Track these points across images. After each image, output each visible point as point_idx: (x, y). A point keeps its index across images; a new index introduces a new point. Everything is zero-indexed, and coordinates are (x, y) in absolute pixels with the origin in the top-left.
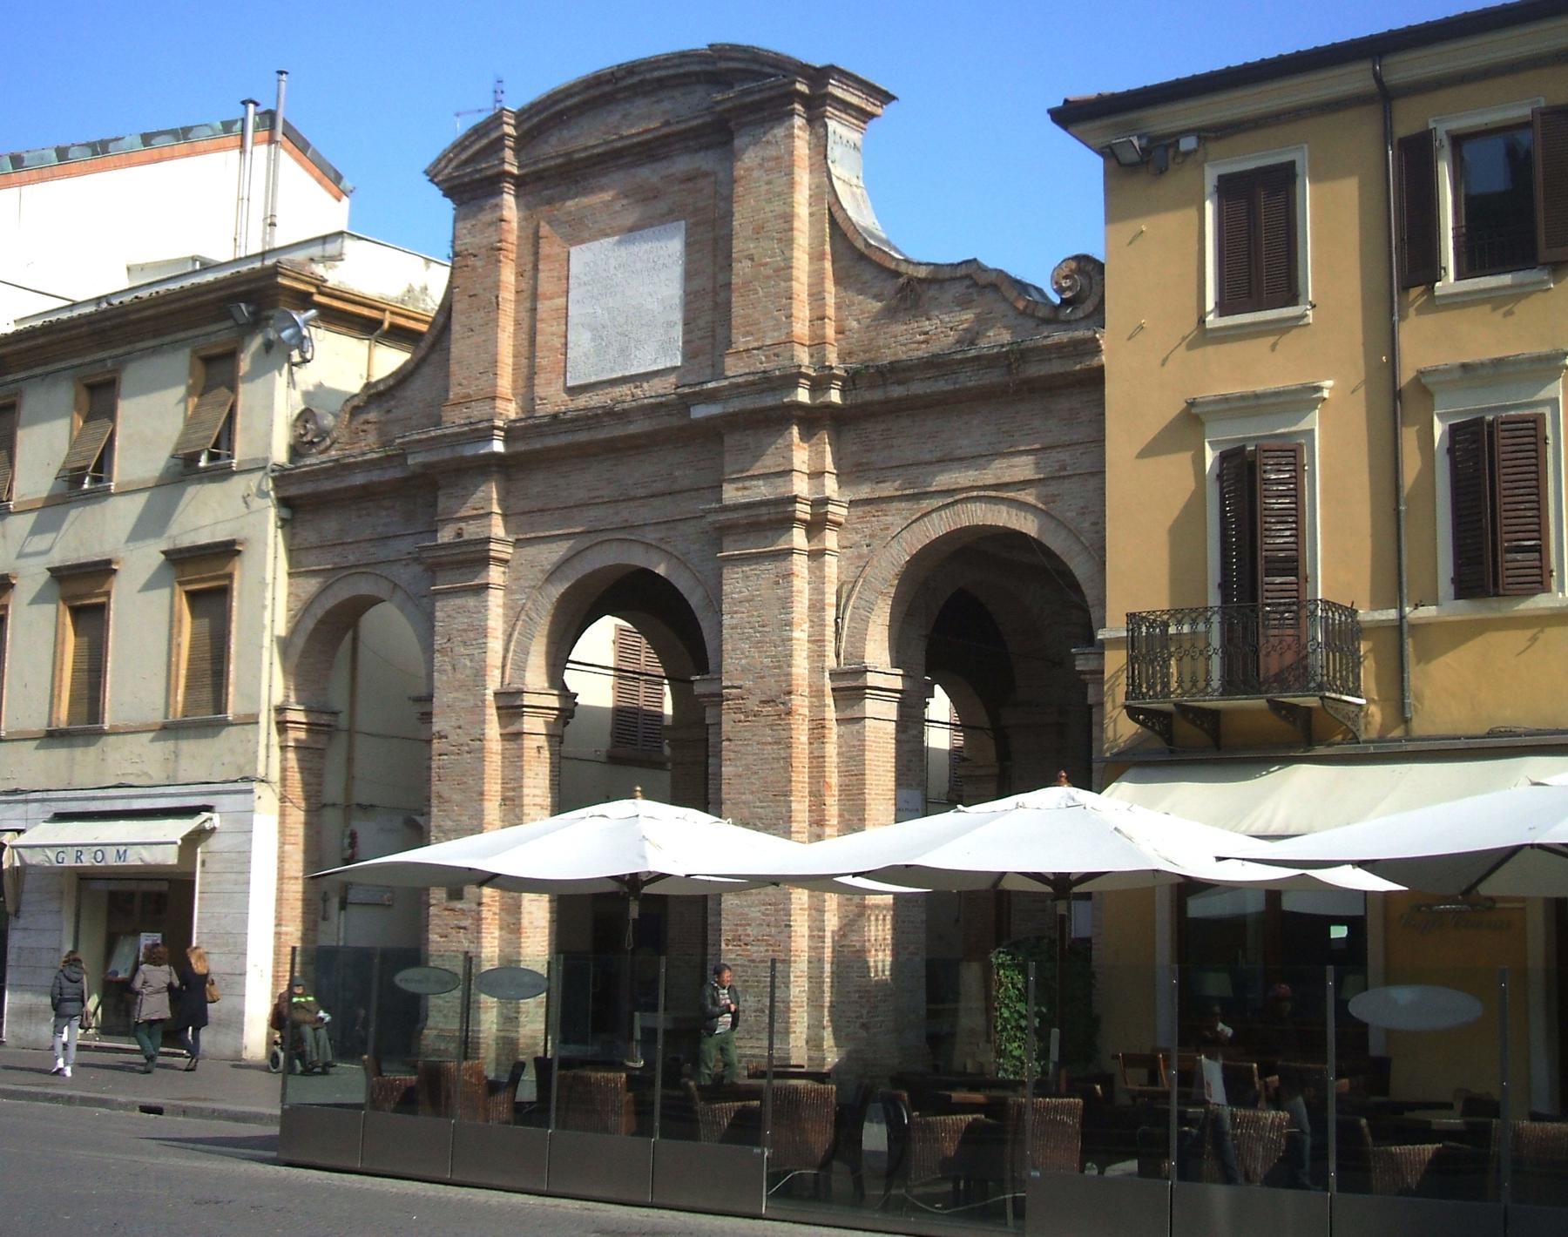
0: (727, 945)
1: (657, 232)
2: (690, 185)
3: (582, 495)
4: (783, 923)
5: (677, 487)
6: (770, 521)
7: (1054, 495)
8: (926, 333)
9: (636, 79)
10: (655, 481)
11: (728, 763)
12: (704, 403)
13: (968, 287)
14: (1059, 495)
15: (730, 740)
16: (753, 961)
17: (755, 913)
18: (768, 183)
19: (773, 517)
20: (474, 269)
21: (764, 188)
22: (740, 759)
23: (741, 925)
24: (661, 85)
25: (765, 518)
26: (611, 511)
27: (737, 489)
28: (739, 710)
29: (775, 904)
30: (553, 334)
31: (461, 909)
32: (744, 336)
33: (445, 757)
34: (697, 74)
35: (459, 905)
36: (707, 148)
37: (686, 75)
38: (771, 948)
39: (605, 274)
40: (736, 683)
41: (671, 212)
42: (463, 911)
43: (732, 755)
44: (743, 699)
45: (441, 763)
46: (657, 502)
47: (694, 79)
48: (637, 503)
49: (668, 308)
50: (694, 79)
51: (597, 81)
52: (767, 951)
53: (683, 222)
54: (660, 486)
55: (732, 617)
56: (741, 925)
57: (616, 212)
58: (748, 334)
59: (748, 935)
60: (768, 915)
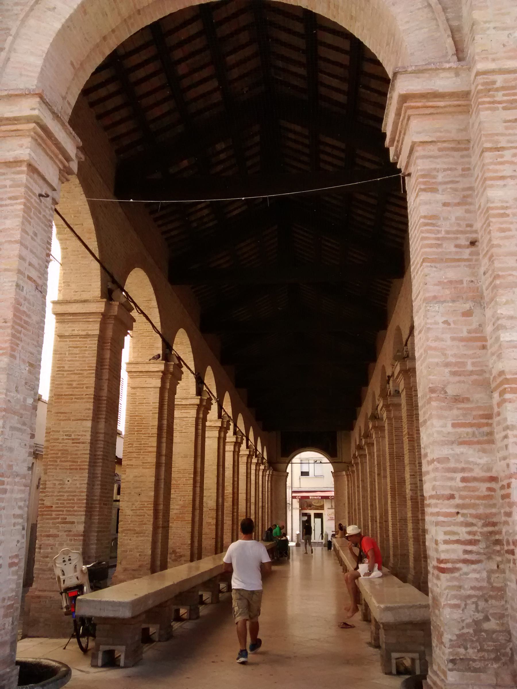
11: (501, 183)
15: (498, 149)
43: (507, 170)
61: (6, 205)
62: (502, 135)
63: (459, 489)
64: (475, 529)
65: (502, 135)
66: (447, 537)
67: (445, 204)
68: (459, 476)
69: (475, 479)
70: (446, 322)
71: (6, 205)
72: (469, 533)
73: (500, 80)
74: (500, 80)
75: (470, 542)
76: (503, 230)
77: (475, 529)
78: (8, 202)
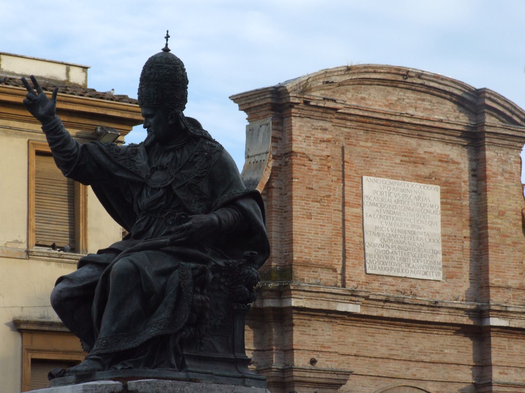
1: (426, 188)
2: (445, 165)
3: (383, 351)
5: (446, 360)
9: (419, 81)
10: (432, 353)
18: (507, 186)
20: (310, 169)
21: (504, 189)
24: (429, 90)
26: (404, 366)
30: (354, 233)
32: (496, 277)
34: (452, 94)
36: (454, 144)
39: (388, 203)
46: (434, 367)
48: (421, 364)
49: (432, 241)
51: (398, 71)
53: (439, 187)
54: (436, 358)
57: (396, 163)
58: (498, 276)
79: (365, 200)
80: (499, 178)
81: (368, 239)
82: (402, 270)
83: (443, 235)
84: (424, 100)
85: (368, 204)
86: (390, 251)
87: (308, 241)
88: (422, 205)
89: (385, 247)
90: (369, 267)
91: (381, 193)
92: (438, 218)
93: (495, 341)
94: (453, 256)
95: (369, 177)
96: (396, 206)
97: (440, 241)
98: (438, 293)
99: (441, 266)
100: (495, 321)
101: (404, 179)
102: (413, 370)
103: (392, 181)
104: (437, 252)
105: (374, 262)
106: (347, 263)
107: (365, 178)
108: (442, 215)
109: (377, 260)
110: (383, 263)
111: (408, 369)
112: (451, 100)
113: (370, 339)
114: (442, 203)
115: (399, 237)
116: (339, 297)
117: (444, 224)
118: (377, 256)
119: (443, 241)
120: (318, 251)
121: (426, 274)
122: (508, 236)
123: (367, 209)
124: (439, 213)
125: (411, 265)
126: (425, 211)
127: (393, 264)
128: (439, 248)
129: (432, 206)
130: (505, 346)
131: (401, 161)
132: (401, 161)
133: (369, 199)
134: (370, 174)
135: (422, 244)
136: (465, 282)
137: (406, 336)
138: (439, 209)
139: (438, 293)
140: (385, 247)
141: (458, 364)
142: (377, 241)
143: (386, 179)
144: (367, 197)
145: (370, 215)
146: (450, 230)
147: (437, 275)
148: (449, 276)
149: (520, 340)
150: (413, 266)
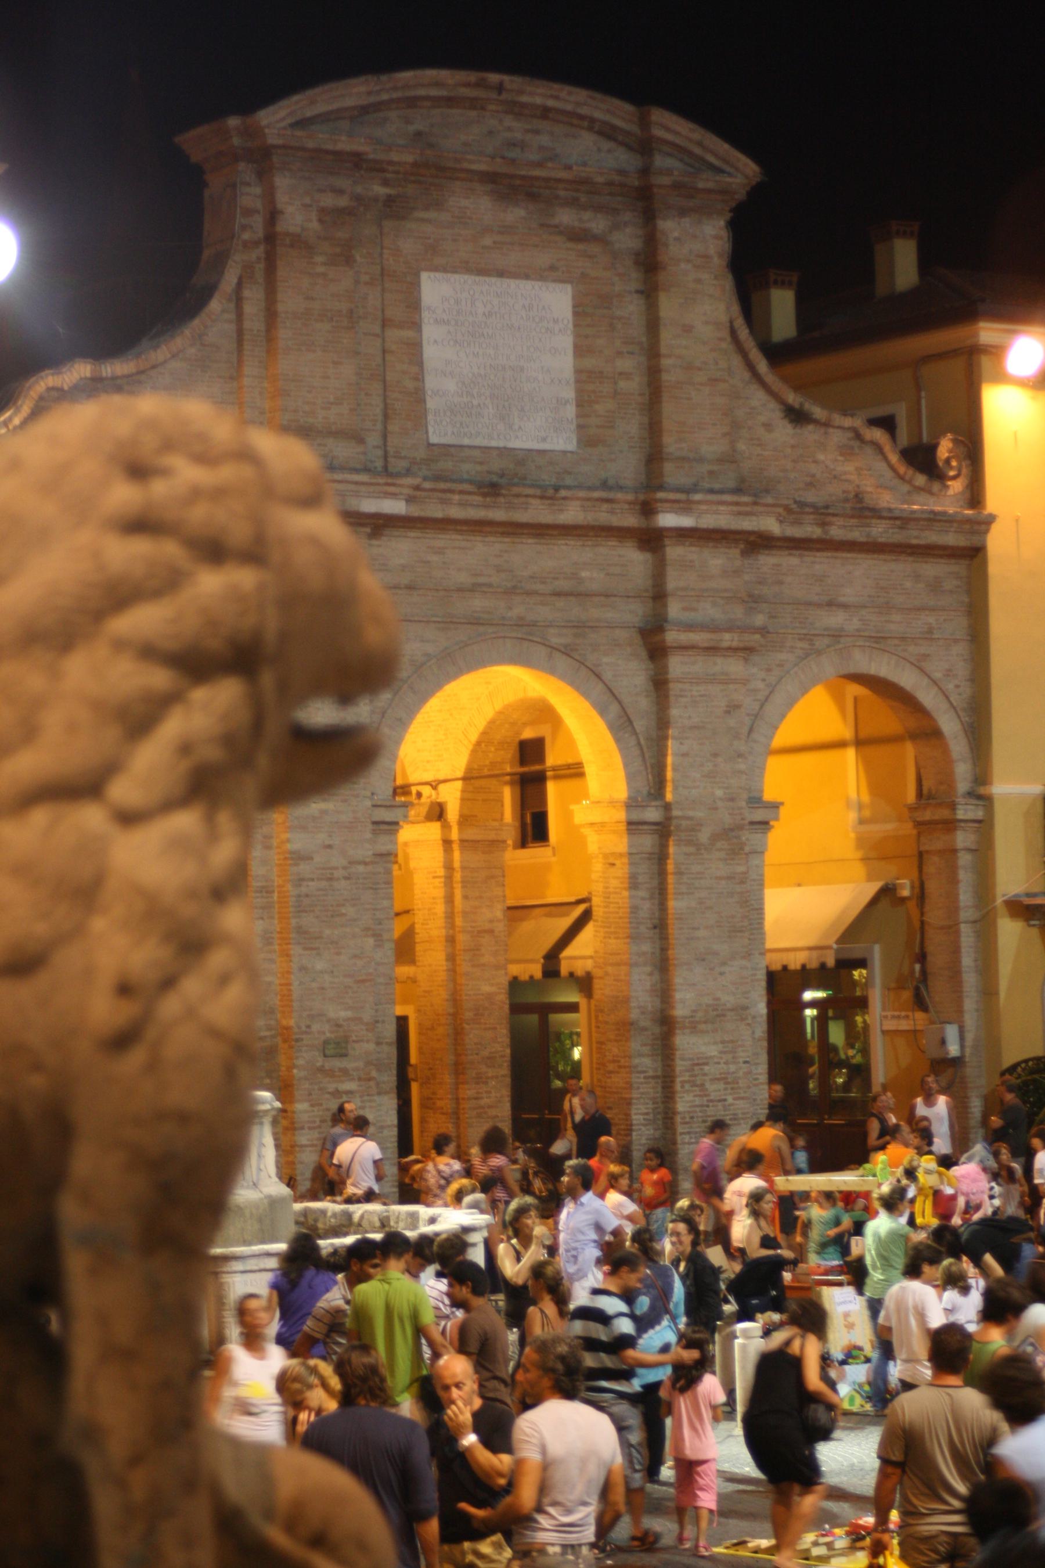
0: (682, 1087)
3: (464, 578)
4: (741, 1060)
6: (730, 648)
7: (924, 655)
8: (813, 476)
12: (676, 513)
13: (850, 439)
14: (928, 655)
16: (711, 1101)
17: (713, 1051)
19: (735, 644)
22: (692, 893)
23: (698, 1064)
25: (725, 644)
27: (685, 609)
28: (689, 843)
29: (732, 1042)
31: (341, 1070)
33: (311, 883)
34: (592, 120)
35: (337, 1063)
37: (582, 117)
38: (729, 1086)
40: (691, 813)
41: (552, 268)
42: (345, 1072)
44: (693, 830)
45: (304, 890)
46: (561, 603)
47: (586, 124)
50: (586, 124)
52: (726, 1089)
55: (681, 744)
56: (698, 1064)
57: (484, 247)
59: (705, 1075)
60: (725, 1052)
61: (382, 889)
62: (683, 864)
63: (642, 1083)
64: (648, 1106)
65: (683, 864)
66: (636, 1111)
67: (643, 899)
68: (642, 1076)
69: (649, 1077)
70: (640, 980)
71: (382, 889)
72: (647, 1108)
73: (684, 823)
74: (684, 823)
75: (647, 1114)
76: (681, 929)
77: (648, 1106)
78: (383, 886)
79: (425, 315)
80: (683, 266)
81: (431, 383)
82: (498, 436)
83: (578, 371)
84: (537, 132)
85: (432, 321)
86: (475, 402)
87: (309, 392)
88: (537, 320)
89: (465, 396)
90: (434, 432)
91: (457, 302)
92: (566, 342)
93: (674, 552)
94: (597, 407)
95: (432, 274)
96: (486, 323)
97: (572, 380)
98: (570, 473)
99: (573, 427)
100: (668, 520)
101: (501, 274)
102: (518, 610)
103: (477, 278)
104: (567, 402)
105: (444, 423)
106: (390, 428)
107: (424, 276)
108: (577, 336)
109: (448, 420)
110: (461, 424)
111: (510, 608)
112: (590, 129)
113: (434, 558)
114: (576, 314)
115: (492, 377)
116: (363, 488)
117: (579, 351)
118: (448, 413)
119: (578, 381)
120: (329, 409)
121: (544, 440)
122: (700, 369)
123: (430, 332)
124: (569, 332)
125: (516, 427)
126: (543, 330)
127: (480, 425)
128: (569, 393)
129: (556, 321)
130: (691, 561)
131: (494, 242)
132: (494, 242)
133: (434, 312)
134: (435, 269)
135: (537, 389)
136: (621, 452)
137: (506, 551)
138: (571, 326)
139: (570, 473)
140: (465, 396)
141: (607, 596)
142: (451, 385)
143: (466, 277)
144: (429, 308)
145: (435, 341)
146: (589, 363)
147: (564, 441)
148: (588, 440)
149: (722, 550)
150: (520, 428)
